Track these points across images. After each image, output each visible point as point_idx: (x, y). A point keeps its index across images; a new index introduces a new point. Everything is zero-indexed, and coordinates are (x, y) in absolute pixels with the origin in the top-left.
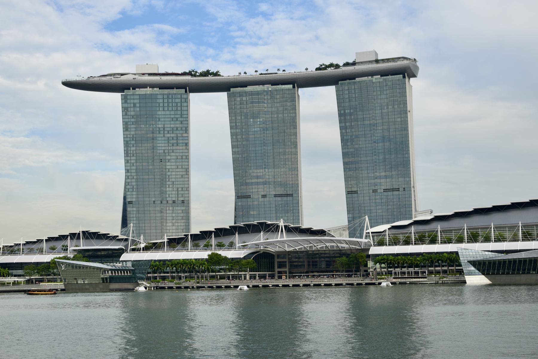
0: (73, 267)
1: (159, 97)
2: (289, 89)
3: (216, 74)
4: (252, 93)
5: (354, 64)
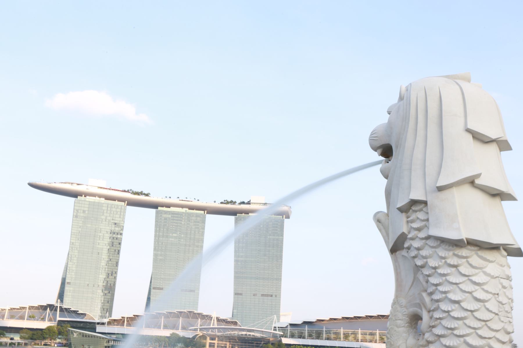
0: (83, 336)
1: (104, 205)
2: (201, 214)
3: (147, 195)
4: (173, 213)
5: (249, 203)
